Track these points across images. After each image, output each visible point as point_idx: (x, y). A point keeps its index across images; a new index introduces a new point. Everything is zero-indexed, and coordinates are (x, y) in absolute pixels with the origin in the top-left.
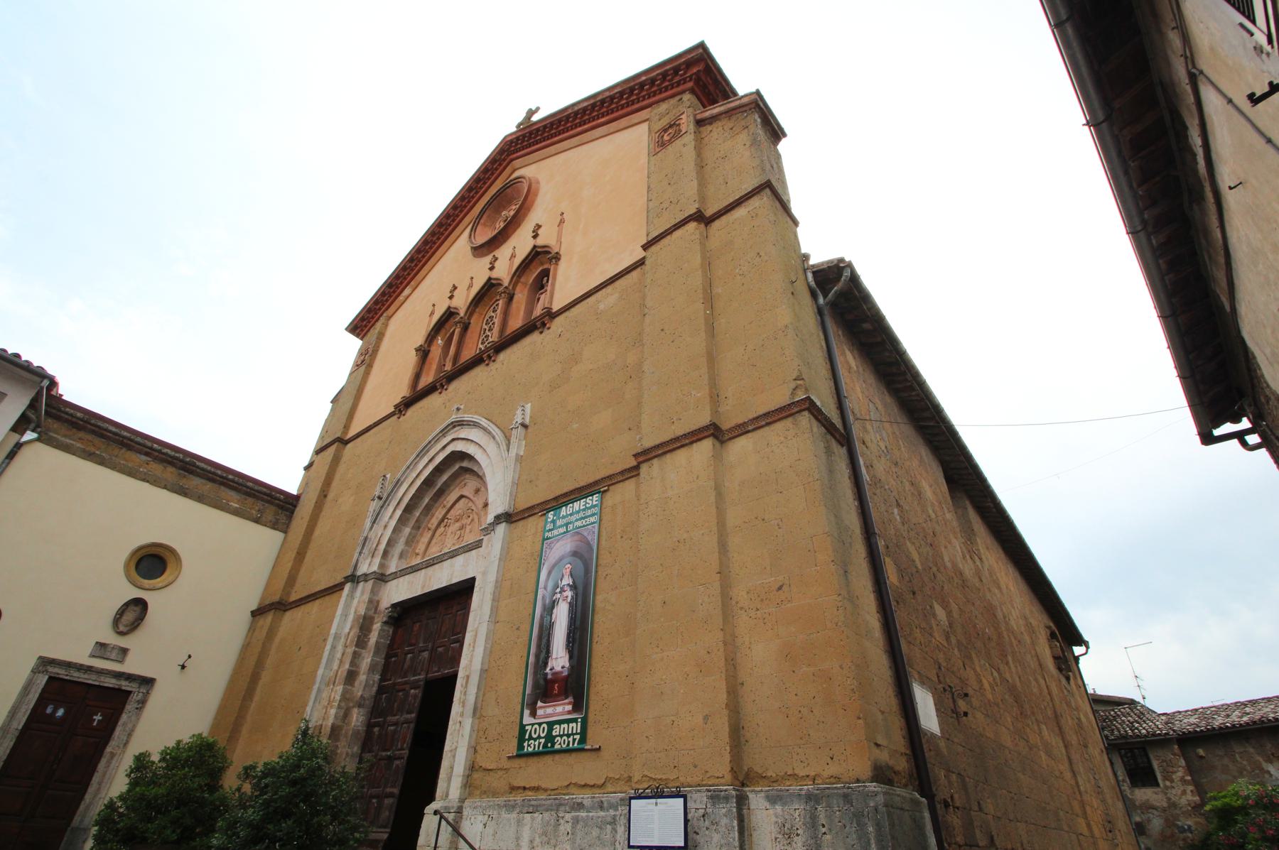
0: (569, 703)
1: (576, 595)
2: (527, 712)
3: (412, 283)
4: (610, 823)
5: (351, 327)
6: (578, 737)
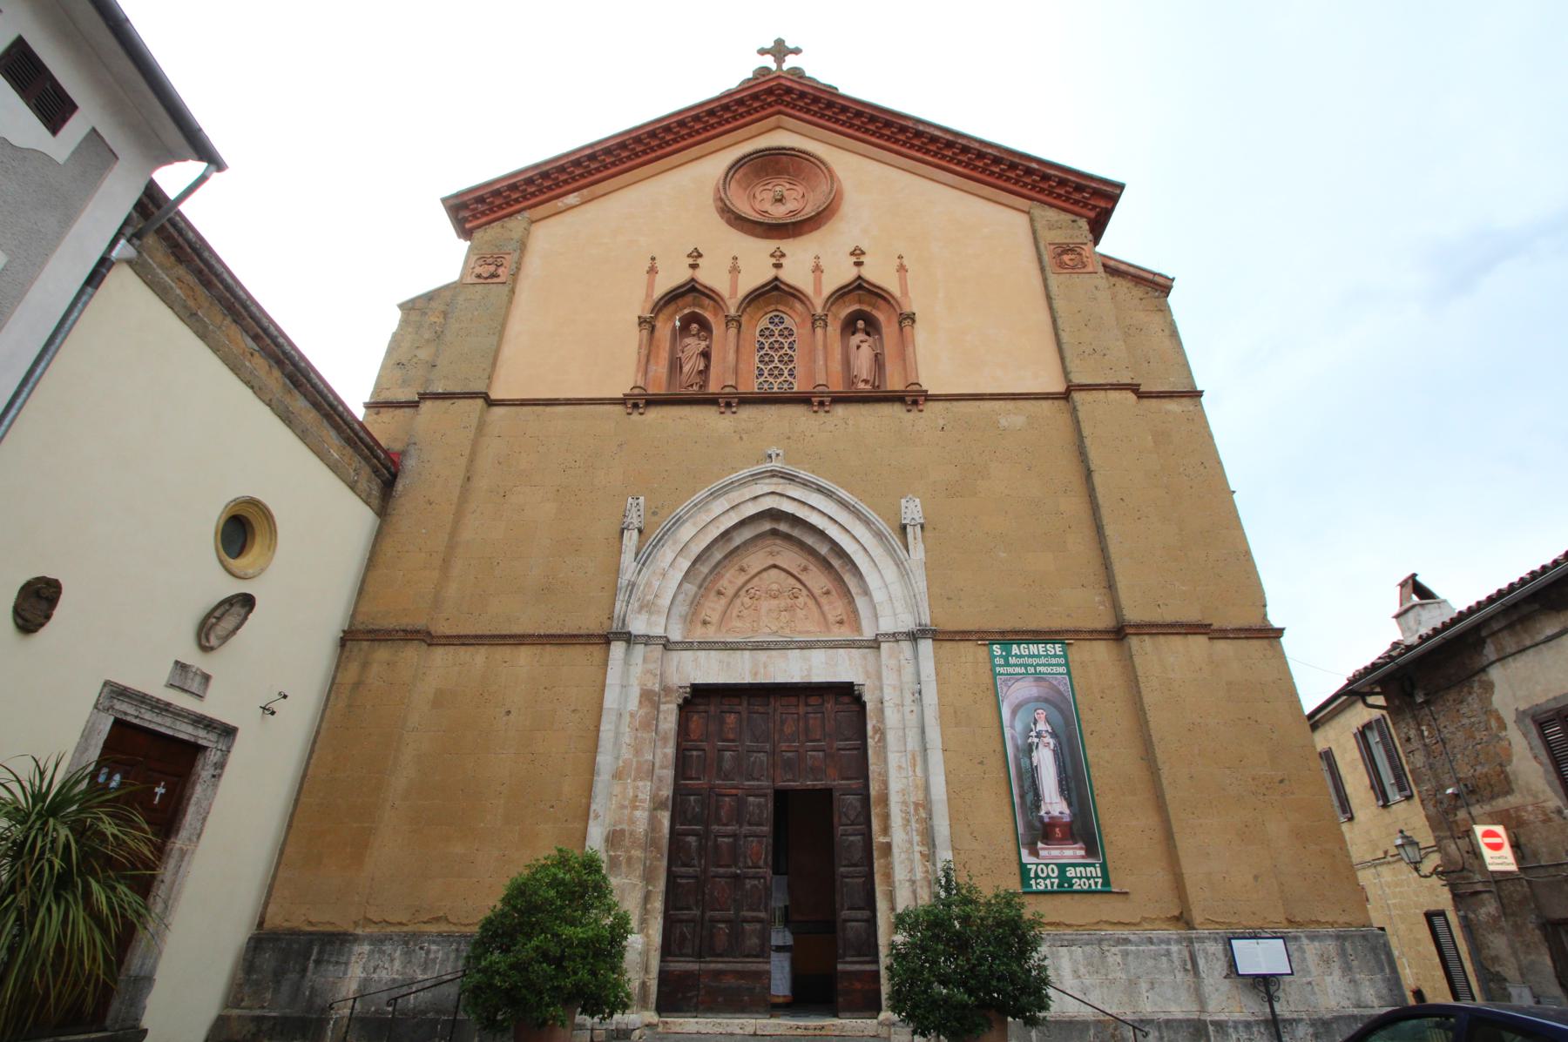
0: (1081, 849)
1: (1060, 744)
2: (1024, 852)
3: (585, 191)
4: (1165, 955)
5: (457, 201)
6: (1100, 881)
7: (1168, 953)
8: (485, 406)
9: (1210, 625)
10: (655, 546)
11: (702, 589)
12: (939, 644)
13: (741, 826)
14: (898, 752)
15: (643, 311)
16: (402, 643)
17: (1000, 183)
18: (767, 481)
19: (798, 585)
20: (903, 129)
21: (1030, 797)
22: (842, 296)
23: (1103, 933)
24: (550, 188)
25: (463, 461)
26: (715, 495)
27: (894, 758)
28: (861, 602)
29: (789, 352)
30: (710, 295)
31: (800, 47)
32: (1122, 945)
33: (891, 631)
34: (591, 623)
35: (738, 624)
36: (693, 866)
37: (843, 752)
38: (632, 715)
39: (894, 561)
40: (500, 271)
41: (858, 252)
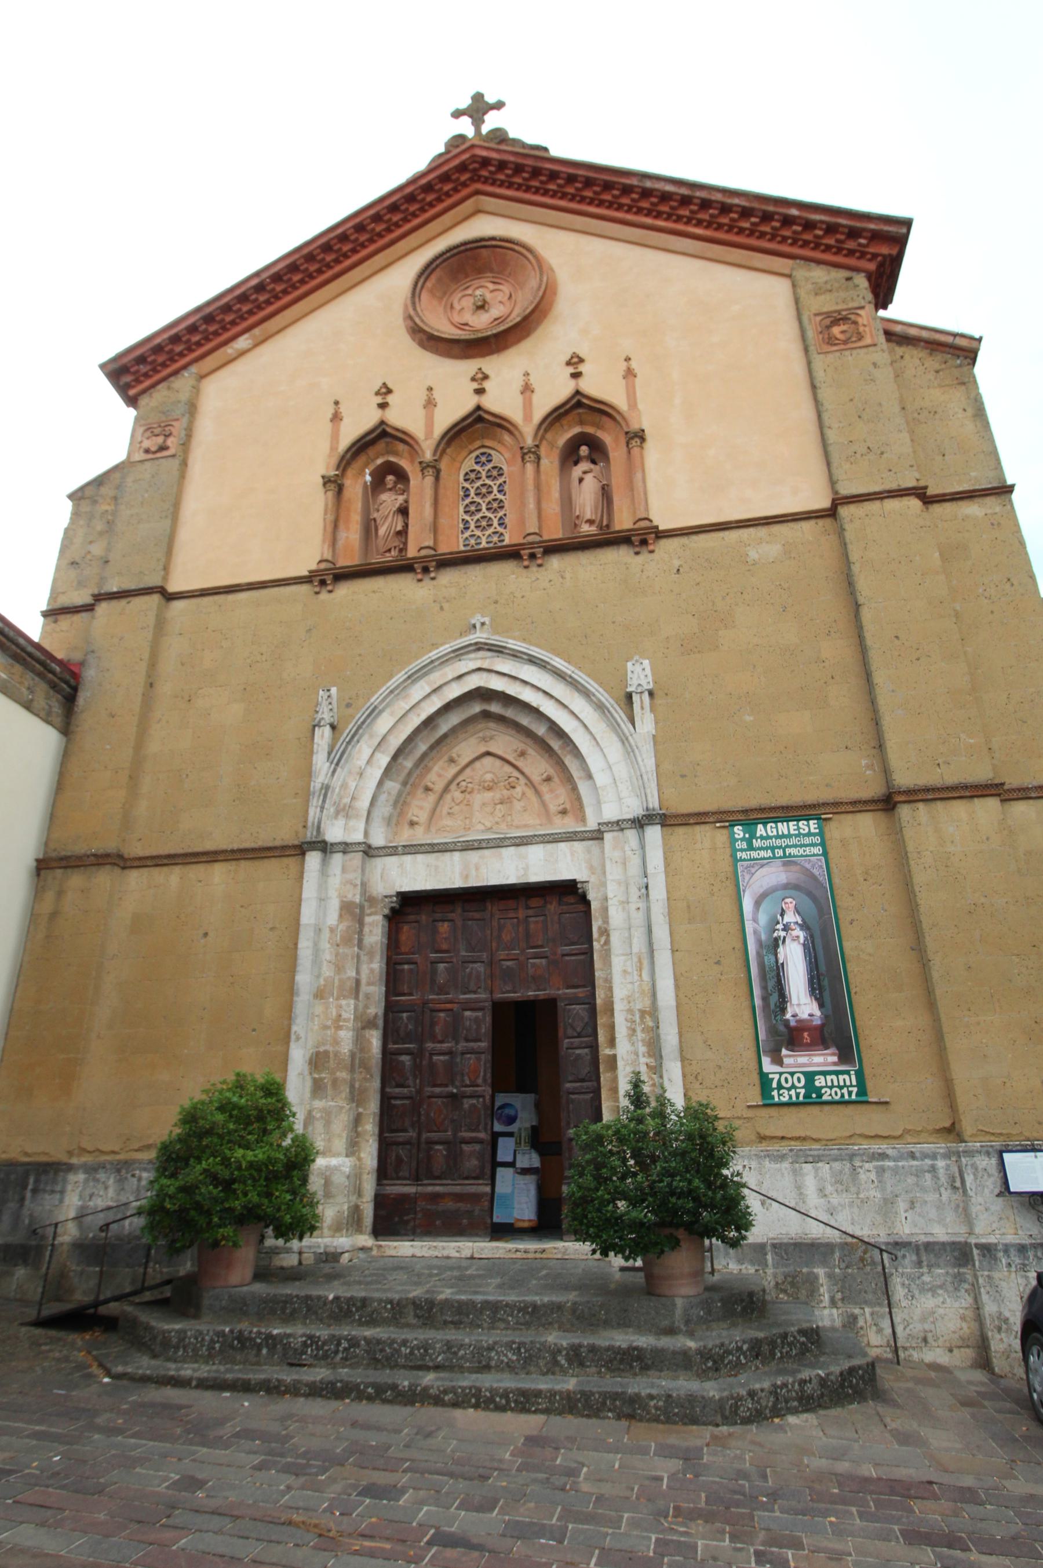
0: (833, 1054)
1: (812, 936)
2: (766, 1061)
3: (256, 331)
4: (929, 1171)
5: (115, 366)
6: (855, 1090)
7: (933, 1169)
8: (163, 601)
9: (1003, 784)
10: (349, 743)
11: (408, 786)
12: (670, 830)
13: (457, 1043)
14: (623, 955)
15: (327, 468)
16: (94, 868)
17: (752, 242)
18: (472, 656)
19: (516, 774)
20: (627, 190)
21: (774, 998)
22: (558, 418)
23: (856, 1148)
24: (216, 334)
25: (143, 667)
26: (413, 678)
27: (618, 963)
28: (583, 787)
29: (500, 496)
31: (503, 99)
32: (878, 1160)
33: (615, 819)
34: (284, 834)
35: (448, 822)
36: (409, 1087)
37: (567, 958)
38: (332, 930)
39: (619, 736)
40: (170, 442)
41: (575, 360)
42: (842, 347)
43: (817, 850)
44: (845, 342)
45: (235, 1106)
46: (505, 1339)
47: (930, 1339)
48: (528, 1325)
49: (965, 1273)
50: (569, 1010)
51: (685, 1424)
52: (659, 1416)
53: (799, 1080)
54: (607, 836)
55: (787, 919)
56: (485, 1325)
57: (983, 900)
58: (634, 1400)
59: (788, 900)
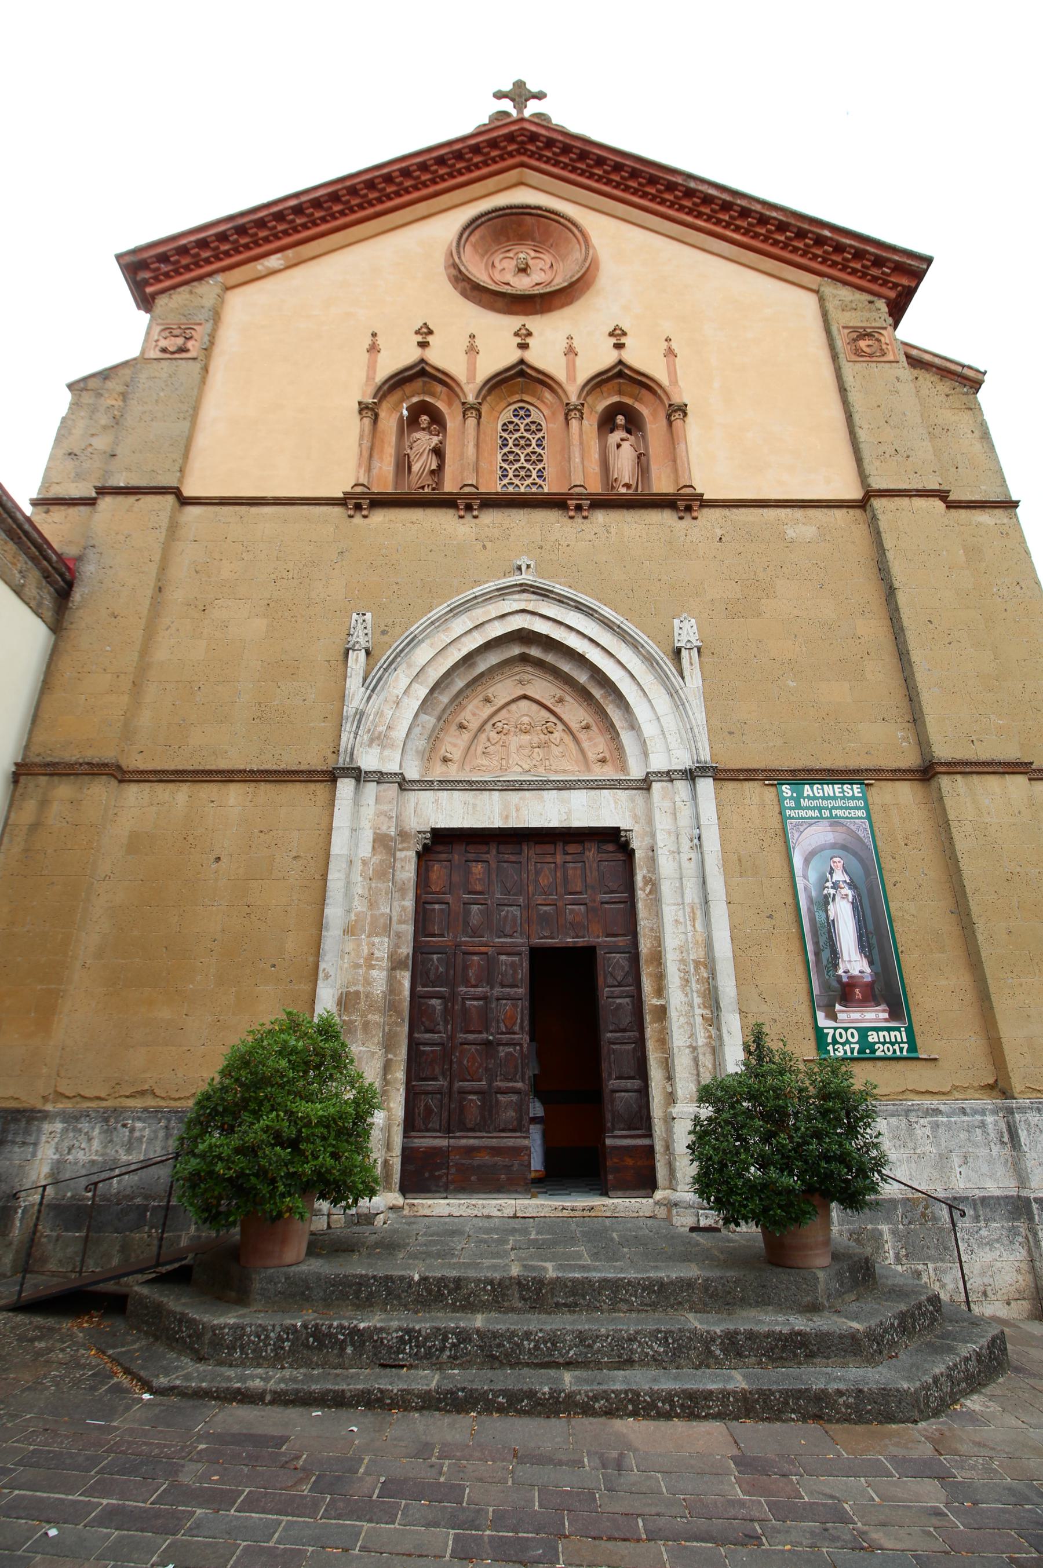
0: (884, 1011)
1: (859, 895)
2: (820, 1015)
3: (290, 253)
4: (979, 1127)
6: (906, 1046)
7: (983, 1125)
8: (177, 504)
9: (1031, 763)
10: (386, 670)
11: (442, 722)
12: (720, 784)
13: (492, 988)
14: (675, 904)
15: (364, 395)
16: (86, 778)
17: (785, 254)
18: (516, 597)
19: (553, 719)
20: (671, 187)
21: (826, 955)
22: (599, 385)
23: (910, 1103)
24: (247, 247)
25: (153, 569)
26: (455, 612)
27: (670, 912)
28: (627, 738)
29: (539, 450)
30: (442, 379)
31: (544, 91)
32: (932, 1116)
33: (665, 769)
34: (313, 758)
35: (485, 762)
36: (440, 1032)
37: (606, 906)
38: (364, 863)
39: (667, 689)
40: (190, 344)
41: (618, 332)
42: (868, 359)
43: (860, 813)
44: (871, 355)
45: (294, 1051)
46: (651, 1327)
47: (989, 1293)
48: (654, 1305)
49: (1018, 1227)
50: (609, 958)
51: (880, 1422)
52: (850, 1414)
53: (852, 1035)
54: (656, 786)
55: (836, 878)
56: (605, 1307)
57: (1018, 869)
58: (821, 1398)
59: (836, 859)
